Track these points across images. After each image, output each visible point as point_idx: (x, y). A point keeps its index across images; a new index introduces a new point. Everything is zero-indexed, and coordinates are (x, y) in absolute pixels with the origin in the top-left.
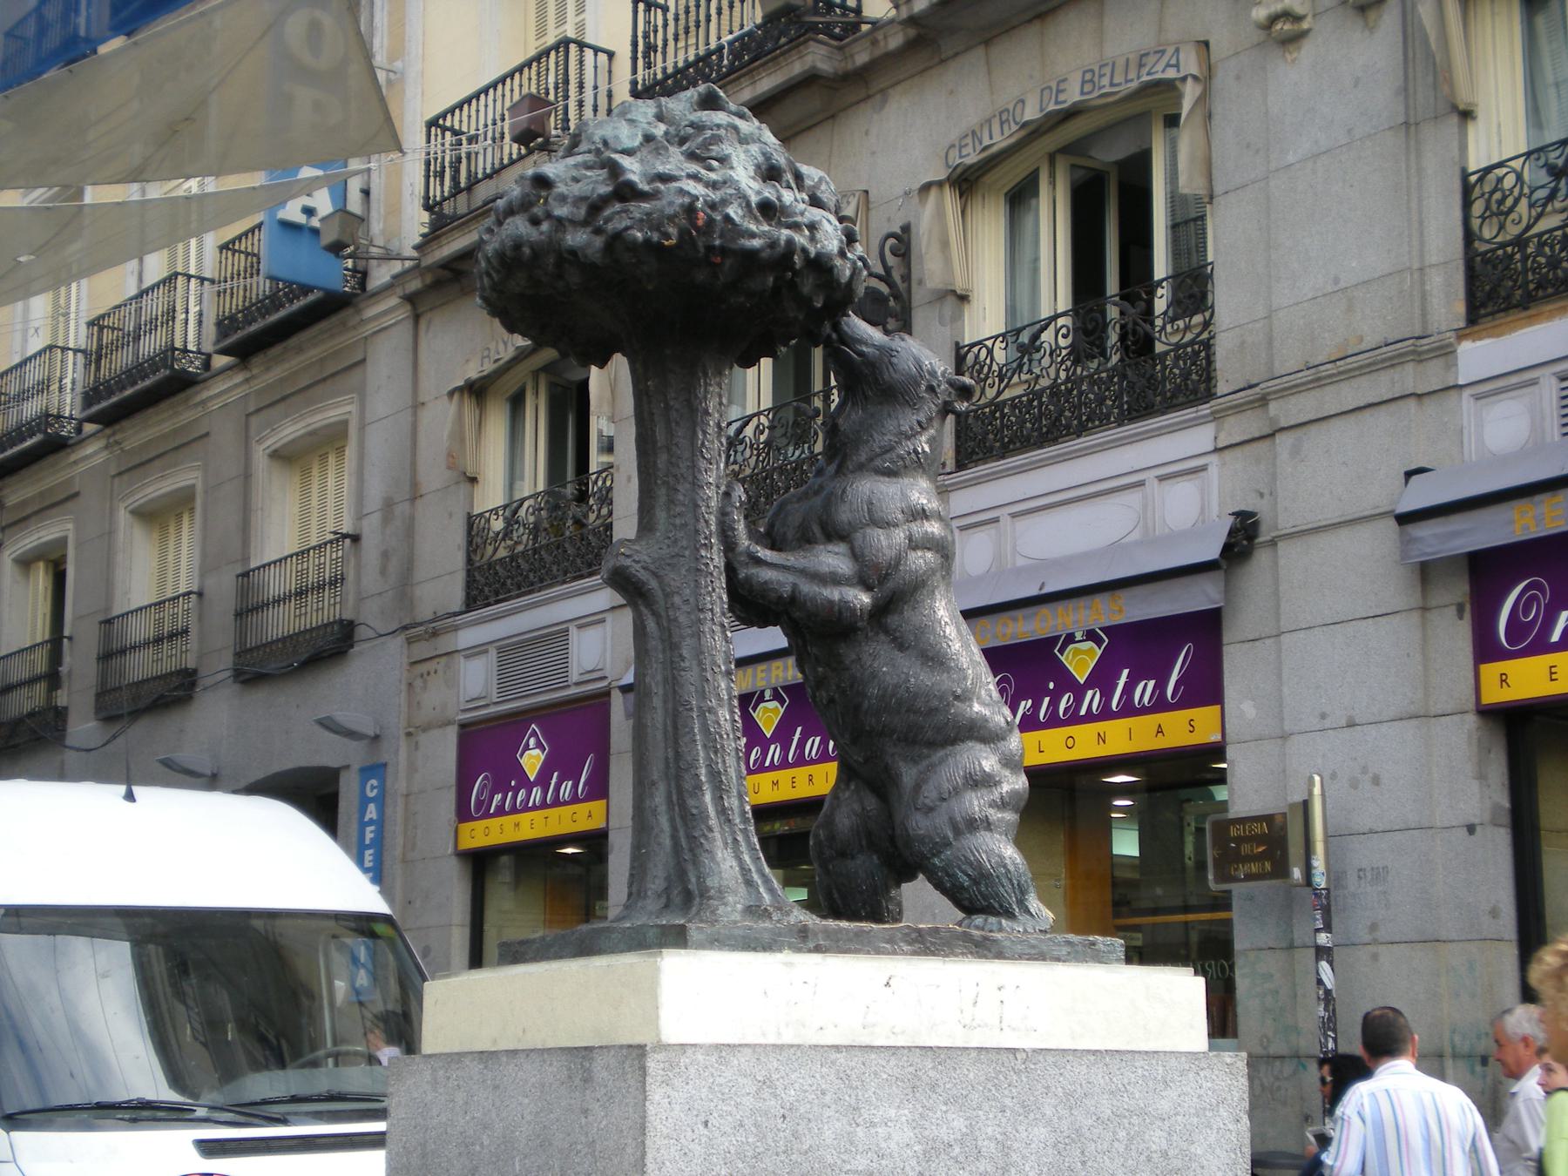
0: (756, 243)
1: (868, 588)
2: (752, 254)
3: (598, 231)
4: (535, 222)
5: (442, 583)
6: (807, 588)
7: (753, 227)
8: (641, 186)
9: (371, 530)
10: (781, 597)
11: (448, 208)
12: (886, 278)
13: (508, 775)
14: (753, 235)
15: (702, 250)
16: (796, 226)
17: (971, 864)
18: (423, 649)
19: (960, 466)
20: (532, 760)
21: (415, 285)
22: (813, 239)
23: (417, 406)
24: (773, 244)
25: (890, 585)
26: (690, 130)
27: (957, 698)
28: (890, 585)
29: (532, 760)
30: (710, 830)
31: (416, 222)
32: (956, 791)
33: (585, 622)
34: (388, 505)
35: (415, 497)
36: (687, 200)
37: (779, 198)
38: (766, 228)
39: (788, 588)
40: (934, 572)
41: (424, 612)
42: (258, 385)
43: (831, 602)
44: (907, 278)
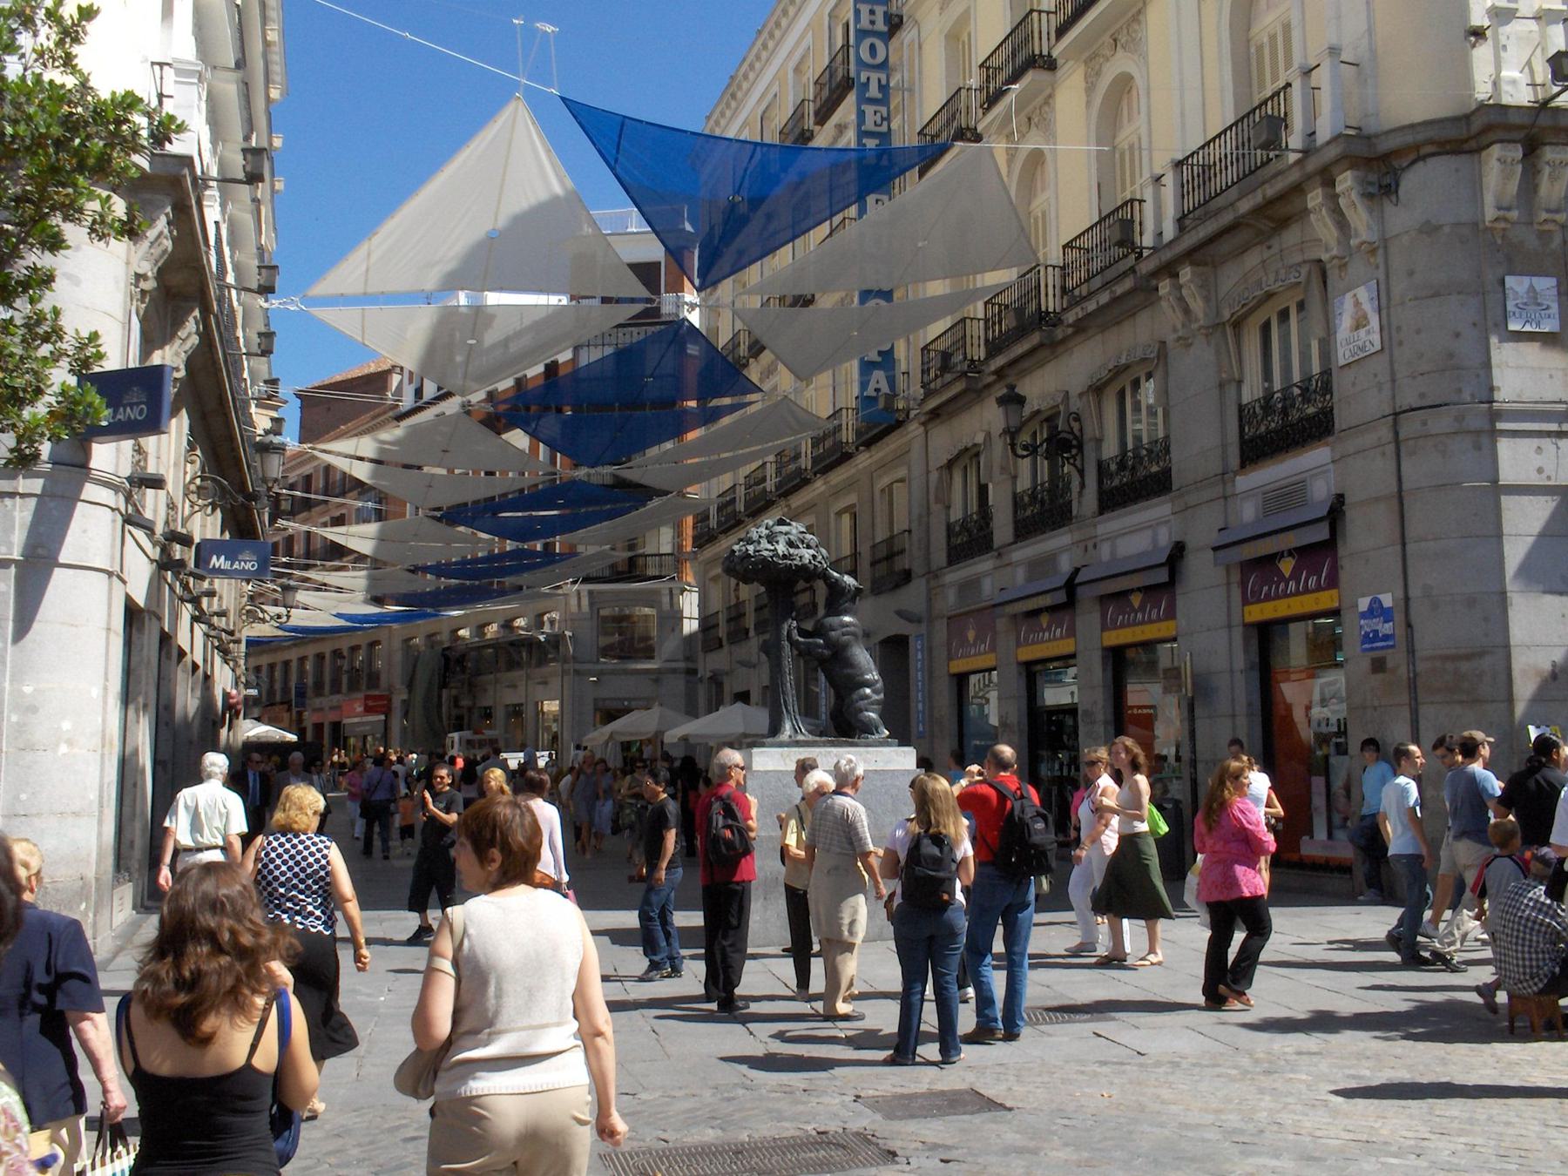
5: (940, 556)
9: (914, 527)
11: (932, 386)
12: (1072, 432)
13: (964, 642)
18: (933, 583)
19: (1101, 513)
20: (971, 635)
21: (923, 419)
23: (928, 472)
29: (971, 635)
31: (917, 390)
33: (986, 574)
34: (920, 516)
35: (928, 514)
41: (934, 567)
42: (875, 458)
44: (1081, 430)
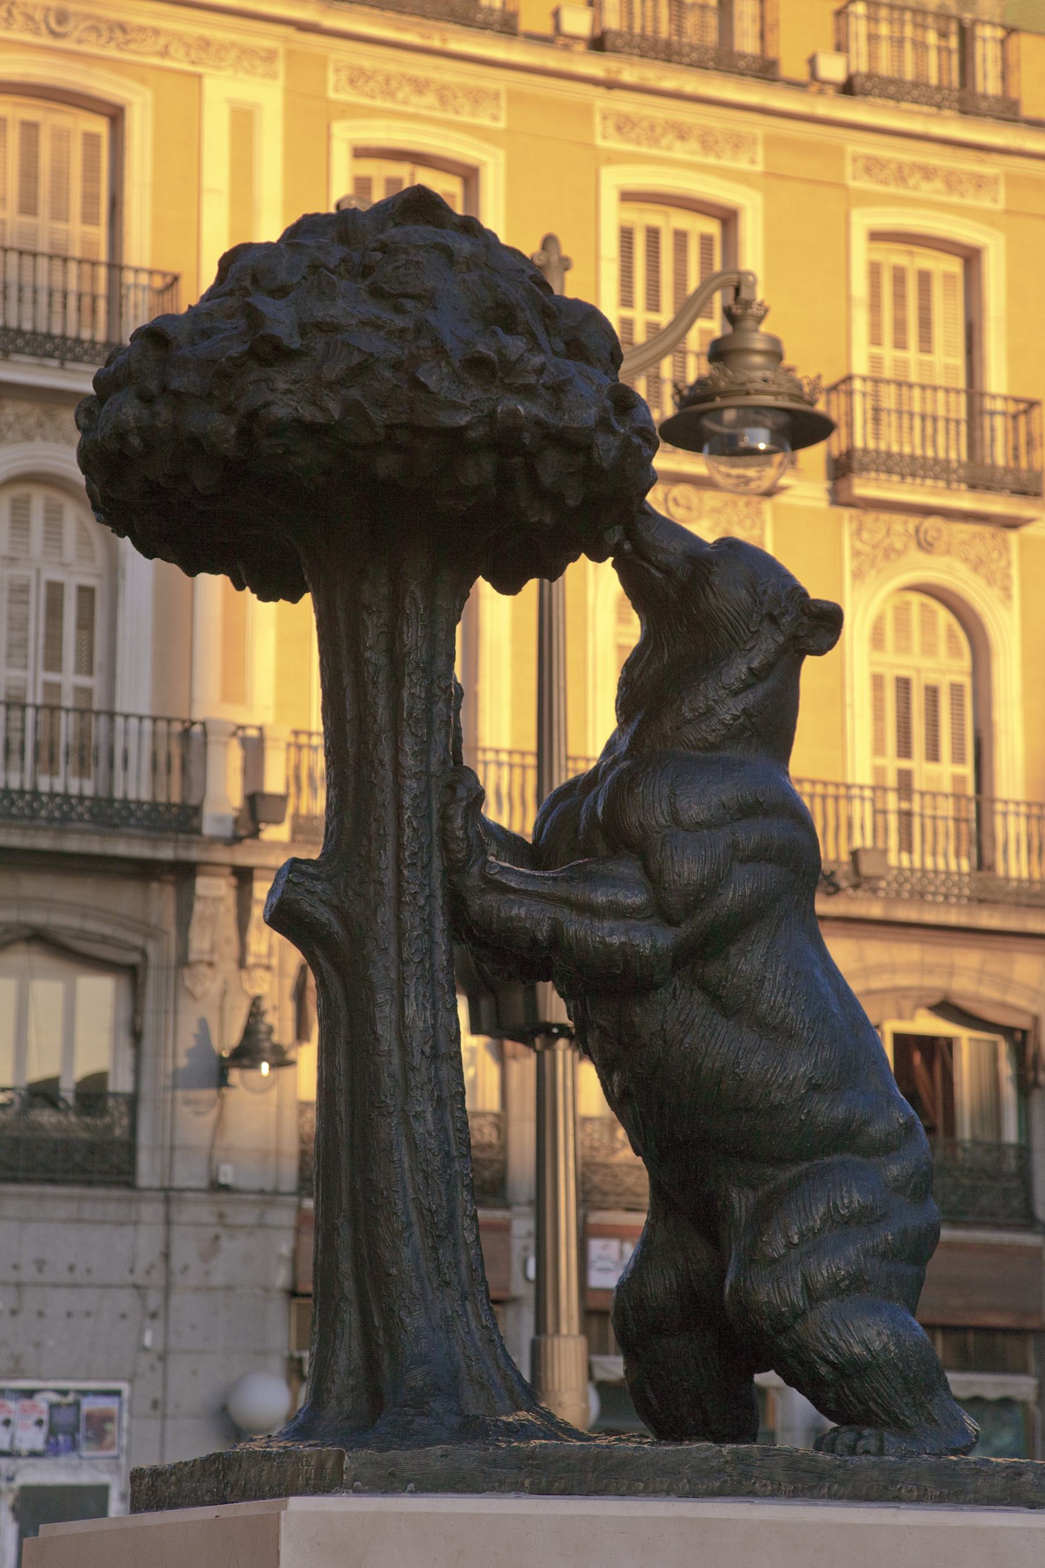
0: (463, 420)
2: (458, 432)
3: (229, 410)
4: (146, 399)
6: (575, 927)
8: (286, 342)
10: (534, 940)
16: (528, 391)
22: (558, 408)
26: (378, 256)
37: (499, 352)
38: (477, 393)
39: (546, 927)
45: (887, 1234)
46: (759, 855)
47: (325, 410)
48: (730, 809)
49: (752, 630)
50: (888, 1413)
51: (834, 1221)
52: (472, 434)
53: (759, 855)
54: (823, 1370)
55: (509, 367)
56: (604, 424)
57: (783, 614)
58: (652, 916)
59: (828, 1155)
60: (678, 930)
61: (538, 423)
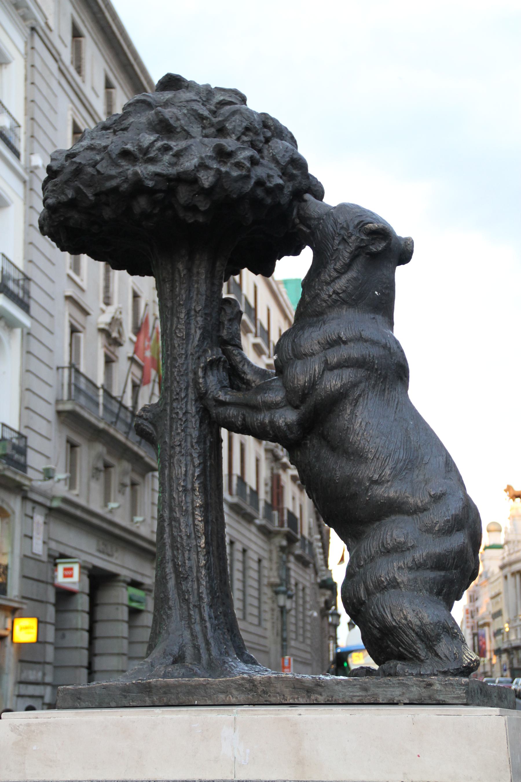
0: (114, 183)
1: (297, 407)
2: (115, 190)
7: (113, 172)
14: (111, 177)
15: (92, 198)
16: (152, 161)
17: (377, 619)
24: (126, 180)
25: (311, 401)
27: (376, 482)
28: (311, 401)
30: (170, 608)
32: (372, 559)
36: (74, 167)
40: (355, 385)
43: (262, 423)
45: (419, 554)
46: (340, 365)
47: (66, 195)
48: (322, 344)
49: (335, 248)
50: (411, 653)
51: (381, 552)
52: (121, 189)
53: (340, 365)
54: (375, 632)
55: (145, 151)
56: (202, 166)
57: (349, 237)
58: (285, 406)
59: (387, 516)
60: (300, 411)
61: (157, 174)
